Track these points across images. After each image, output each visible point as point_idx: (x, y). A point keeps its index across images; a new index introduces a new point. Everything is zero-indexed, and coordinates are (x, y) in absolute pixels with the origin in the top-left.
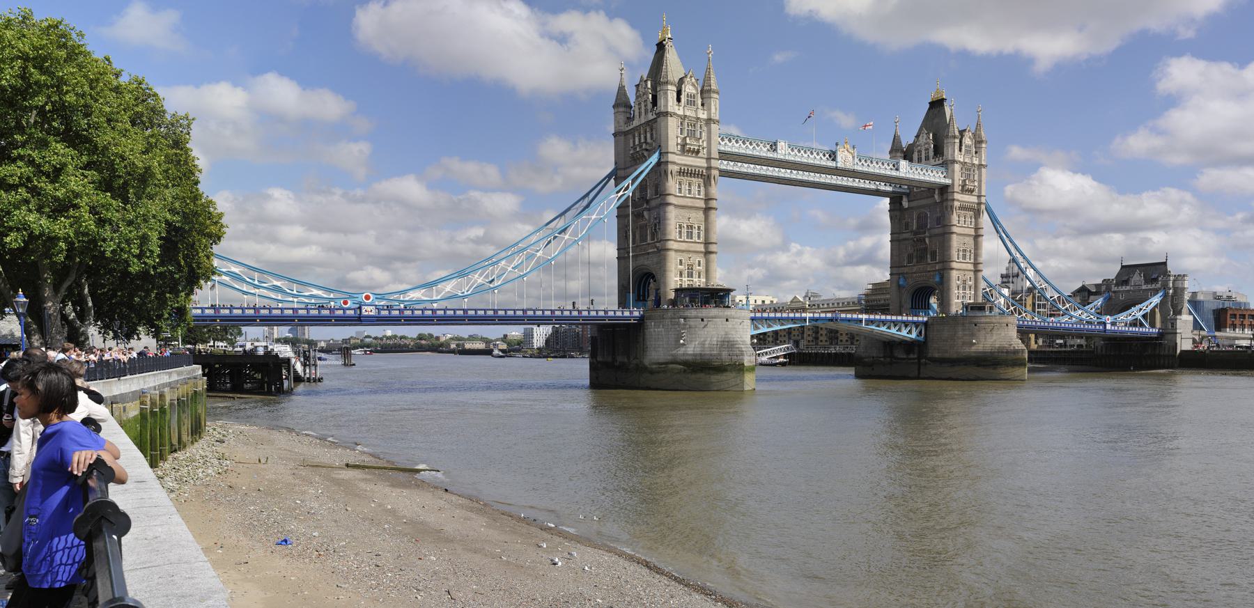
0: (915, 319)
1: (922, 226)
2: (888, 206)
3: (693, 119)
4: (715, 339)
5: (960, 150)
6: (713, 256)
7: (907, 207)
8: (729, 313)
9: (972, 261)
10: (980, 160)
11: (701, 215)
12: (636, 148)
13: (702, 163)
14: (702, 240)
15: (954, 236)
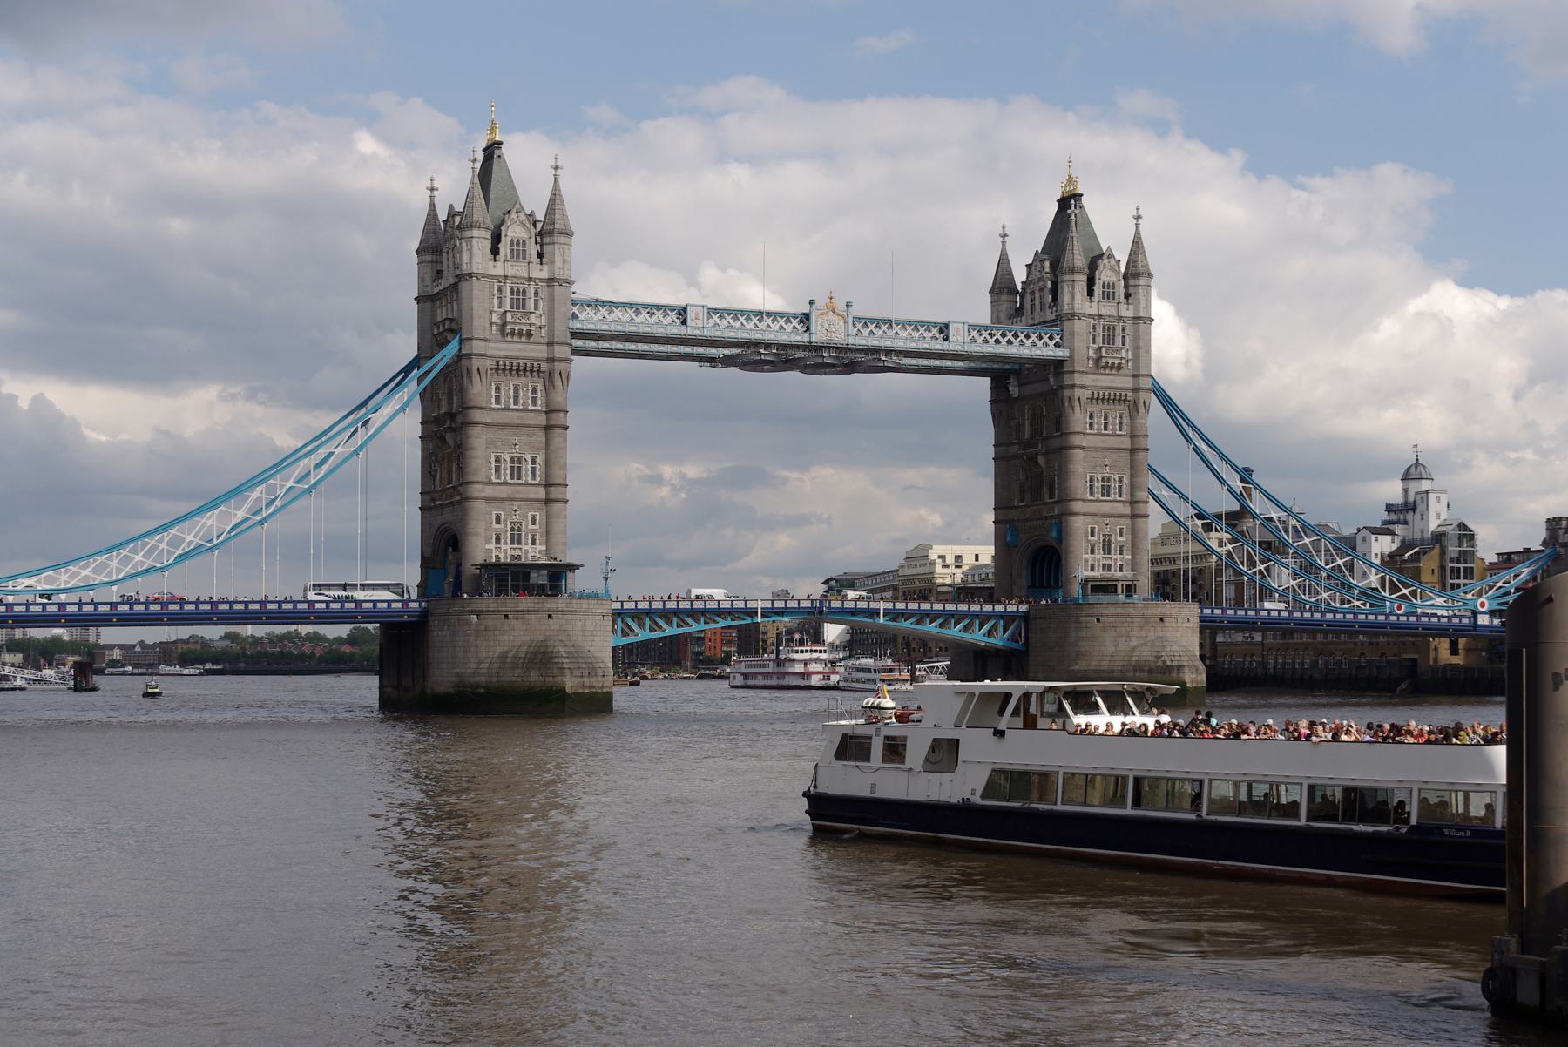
0: (1000, 608)
1: (1036, 432)
2: (987, 394)
3: (522, 281)
4: (524, 649)
5: (1090, 293)
6: (556, 507)
7: (1016, 396)
8: (554, 606)
9: (1125, 497)
10: (1137, 309)
11: (540, 436)
12: (439, 327)
13: (541, 352)
14: (539, 479)
15: (1078, 455)
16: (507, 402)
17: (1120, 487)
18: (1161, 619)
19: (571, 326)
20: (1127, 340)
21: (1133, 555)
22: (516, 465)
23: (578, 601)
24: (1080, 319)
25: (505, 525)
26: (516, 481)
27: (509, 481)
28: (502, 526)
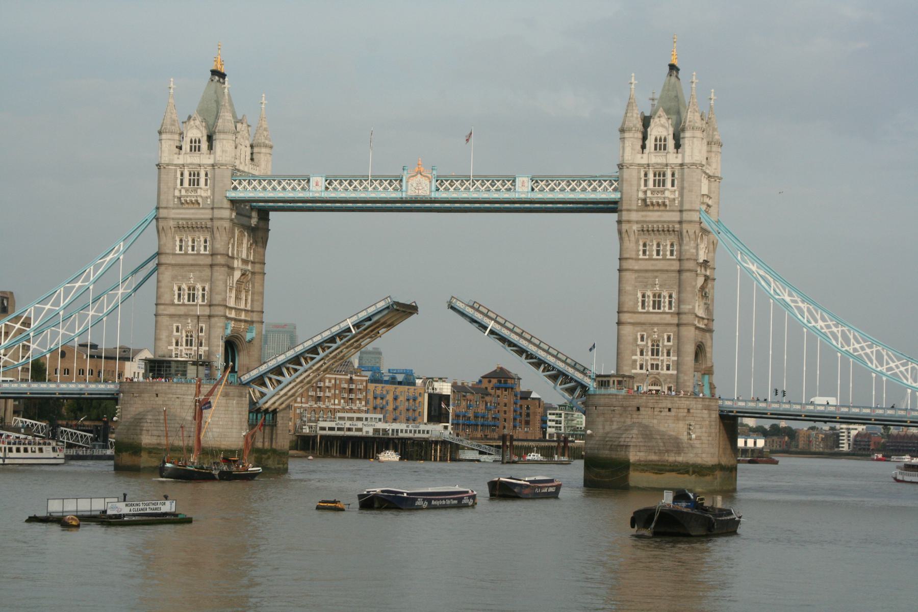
5: (643, 147)
8: (159, 388)
11: (207, 272)
16: (187, 250)
17: (670, 303)
18: (638, 409)
19: (227, 195)
20: (676, 182)
21: (678, 356)
22: (192, 292)
23: (179, 385)
24: (628, 168)
25: (182, 333)
26: (191, 303)
27: (186, 302)
28: (179, 334)
